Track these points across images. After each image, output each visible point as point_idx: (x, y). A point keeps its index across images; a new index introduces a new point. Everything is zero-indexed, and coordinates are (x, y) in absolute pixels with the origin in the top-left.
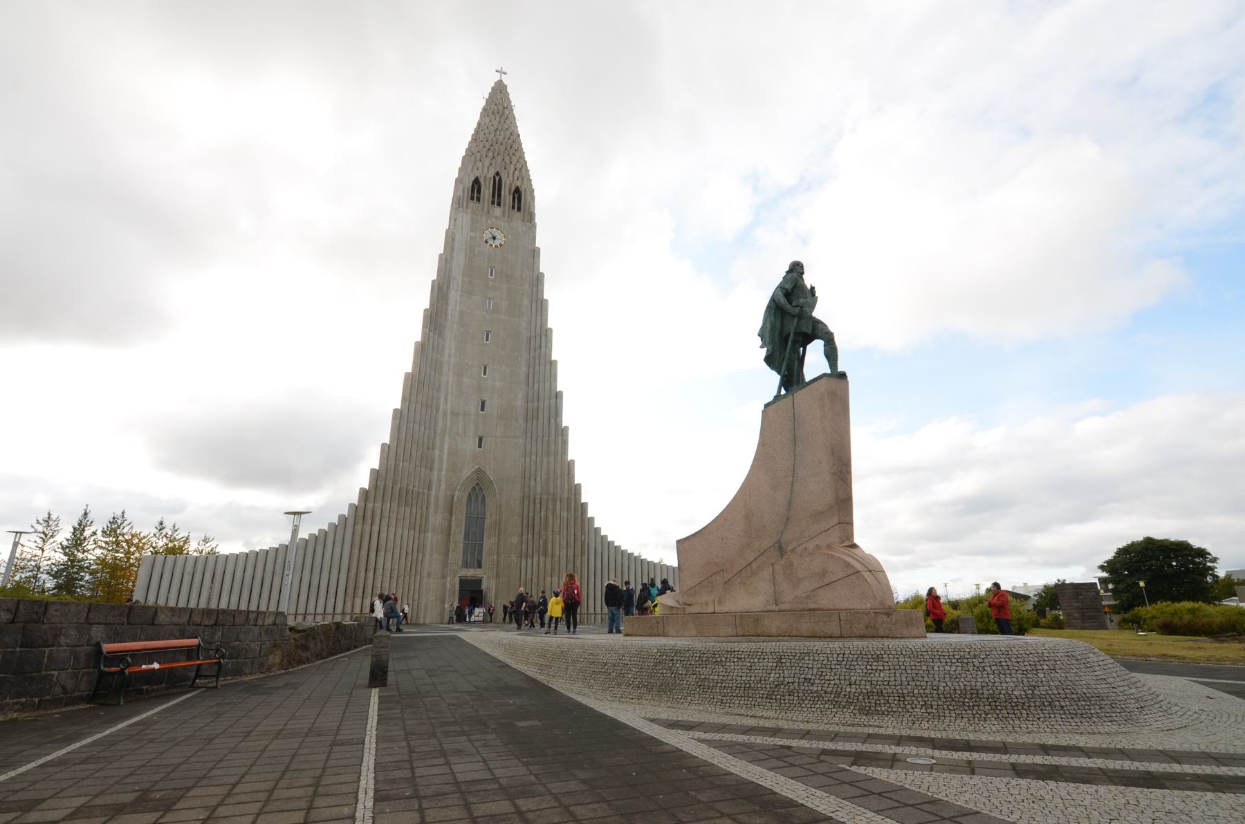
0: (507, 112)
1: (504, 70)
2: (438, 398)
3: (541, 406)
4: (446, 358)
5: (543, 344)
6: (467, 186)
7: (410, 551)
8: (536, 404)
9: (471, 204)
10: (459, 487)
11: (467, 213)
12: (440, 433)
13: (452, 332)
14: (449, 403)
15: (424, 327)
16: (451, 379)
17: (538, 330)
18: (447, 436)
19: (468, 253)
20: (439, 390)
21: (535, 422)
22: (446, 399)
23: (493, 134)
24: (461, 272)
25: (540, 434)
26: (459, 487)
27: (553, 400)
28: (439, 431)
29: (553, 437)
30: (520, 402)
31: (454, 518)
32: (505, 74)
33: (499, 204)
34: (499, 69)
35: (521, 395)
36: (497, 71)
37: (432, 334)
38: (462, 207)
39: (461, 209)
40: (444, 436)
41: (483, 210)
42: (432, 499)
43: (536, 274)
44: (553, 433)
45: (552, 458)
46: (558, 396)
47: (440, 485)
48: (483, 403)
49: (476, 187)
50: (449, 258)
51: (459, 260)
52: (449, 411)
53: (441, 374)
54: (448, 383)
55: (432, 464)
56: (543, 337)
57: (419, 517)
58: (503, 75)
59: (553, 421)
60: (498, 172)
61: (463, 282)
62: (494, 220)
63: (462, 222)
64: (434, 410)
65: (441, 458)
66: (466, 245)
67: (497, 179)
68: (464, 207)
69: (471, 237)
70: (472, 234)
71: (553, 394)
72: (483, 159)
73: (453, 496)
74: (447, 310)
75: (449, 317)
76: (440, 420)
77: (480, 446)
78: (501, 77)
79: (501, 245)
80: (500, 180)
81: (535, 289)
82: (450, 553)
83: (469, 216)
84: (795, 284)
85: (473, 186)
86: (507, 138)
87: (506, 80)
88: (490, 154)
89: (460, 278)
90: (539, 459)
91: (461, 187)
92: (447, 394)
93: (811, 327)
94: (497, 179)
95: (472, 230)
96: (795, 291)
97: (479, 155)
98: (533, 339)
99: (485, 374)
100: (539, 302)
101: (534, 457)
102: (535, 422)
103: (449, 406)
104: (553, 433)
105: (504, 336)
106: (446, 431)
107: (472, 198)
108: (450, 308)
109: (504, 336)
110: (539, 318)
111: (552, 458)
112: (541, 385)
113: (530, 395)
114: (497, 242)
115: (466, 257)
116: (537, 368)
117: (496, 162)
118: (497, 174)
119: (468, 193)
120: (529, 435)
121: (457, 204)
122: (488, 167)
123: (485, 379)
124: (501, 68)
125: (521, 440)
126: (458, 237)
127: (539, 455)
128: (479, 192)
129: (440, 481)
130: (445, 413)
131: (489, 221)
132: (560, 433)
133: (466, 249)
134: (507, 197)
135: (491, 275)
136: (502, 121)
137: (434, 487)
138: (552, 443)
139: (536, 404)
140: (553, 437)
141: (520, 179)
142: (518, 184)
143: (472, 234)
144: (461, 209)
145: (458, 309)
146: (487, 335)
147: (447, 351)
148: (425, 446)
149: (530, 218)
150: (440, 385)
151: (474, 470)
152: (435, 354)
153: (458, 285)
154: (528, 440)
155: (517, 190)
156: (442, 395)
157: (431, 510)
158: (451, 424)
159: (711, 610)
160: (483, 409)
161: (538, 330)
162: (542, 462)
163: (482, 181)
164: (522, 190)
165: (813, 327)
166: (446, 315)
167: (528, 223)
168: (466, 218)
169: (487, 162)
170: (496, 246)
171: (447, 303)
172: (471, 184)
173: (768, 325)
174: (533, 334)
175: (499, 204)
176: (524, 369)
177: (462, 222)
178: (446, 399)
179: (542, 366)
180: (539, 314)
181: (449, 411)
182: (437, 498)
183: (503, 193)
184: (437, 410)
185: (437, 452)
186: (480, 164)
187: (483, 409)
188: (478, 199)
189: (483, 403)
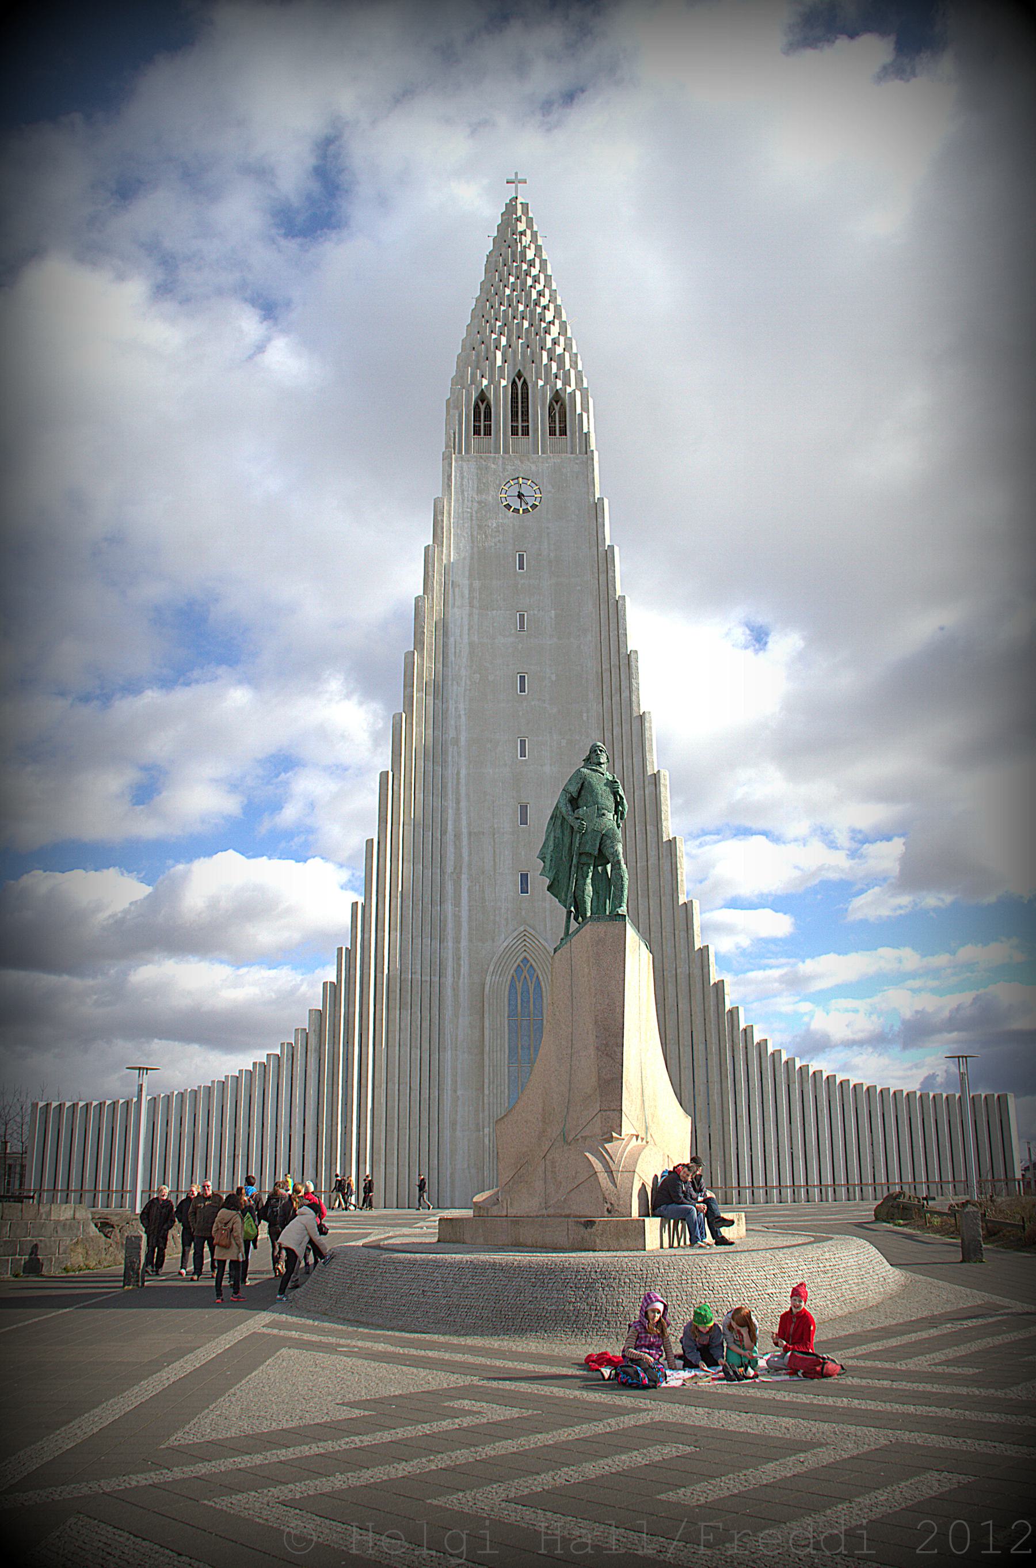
1: (519, 178)
2: (444, 810)
4: (452, 733)
7: (416, 1086)
9: (473, 440)
10: (491, 968)
14: (464, 817)
16: (463, 772)
17: (614, 660)
18: (464, 877)
24: (467, 574)
26: (491, 968)
28: (449, 869)
29: (652, 861)
31: (487, 1024)
38: (460, 452)
40: (459, 878)
42: (449, 992)
44: (652, 853)
47: (459, 965)
48: (524, 809)
49: (482, 407)
52: (465, 831)
53: (444, 764)
54: (458, 779)
55: (443, 929)
57: (426, 1024)
58: (519, 185)
61: (471, 589)
65: (457, 917)
67: (520, 384)
69: (479, 503)
73: (484, 985)
76: (450, 849)
77: (524, 890)
79: (534, 506)
81: (602, 577)
82: (486, 1086)
83: (473, 464)
92: (458, 802)
93: (598, 845)
94: (520, 384)
95: (479, 491)
96: (583, 793)
98: (606, 675)
99: (523, 755)
103: (464, 823)
104: (652, 853)
105: (554, 678)
106: (461, 867)
108: (452, 640)
112: (627, 762)
118: (519, 375)
124: (516, 174)
128: (488, 416)
129: (459, 959)
130: (457, 836)
135: (521, 567)
137: (449, 971)
140: (652, 861)
142: (559, 384)
145: (466, 640)
148: (427, 899)
150: (444, 787)
151: (516, 934)
155: (557, 398)
156: (451, 804)
157: (448, 1013)
158: (470, 854)
159: (504, 1213)
160: (524, 821)
161: (614, 660)
165: (600, 844)
170: (525, 511)
173: (551, 843)
177: (462, 478)
180: (613, 626)
181: (465, 831)
182: (455, 989)
184: (443, 833)
185: (449, 907)
187: (524, 821)
188: (488, 432)
189: (524, 809)
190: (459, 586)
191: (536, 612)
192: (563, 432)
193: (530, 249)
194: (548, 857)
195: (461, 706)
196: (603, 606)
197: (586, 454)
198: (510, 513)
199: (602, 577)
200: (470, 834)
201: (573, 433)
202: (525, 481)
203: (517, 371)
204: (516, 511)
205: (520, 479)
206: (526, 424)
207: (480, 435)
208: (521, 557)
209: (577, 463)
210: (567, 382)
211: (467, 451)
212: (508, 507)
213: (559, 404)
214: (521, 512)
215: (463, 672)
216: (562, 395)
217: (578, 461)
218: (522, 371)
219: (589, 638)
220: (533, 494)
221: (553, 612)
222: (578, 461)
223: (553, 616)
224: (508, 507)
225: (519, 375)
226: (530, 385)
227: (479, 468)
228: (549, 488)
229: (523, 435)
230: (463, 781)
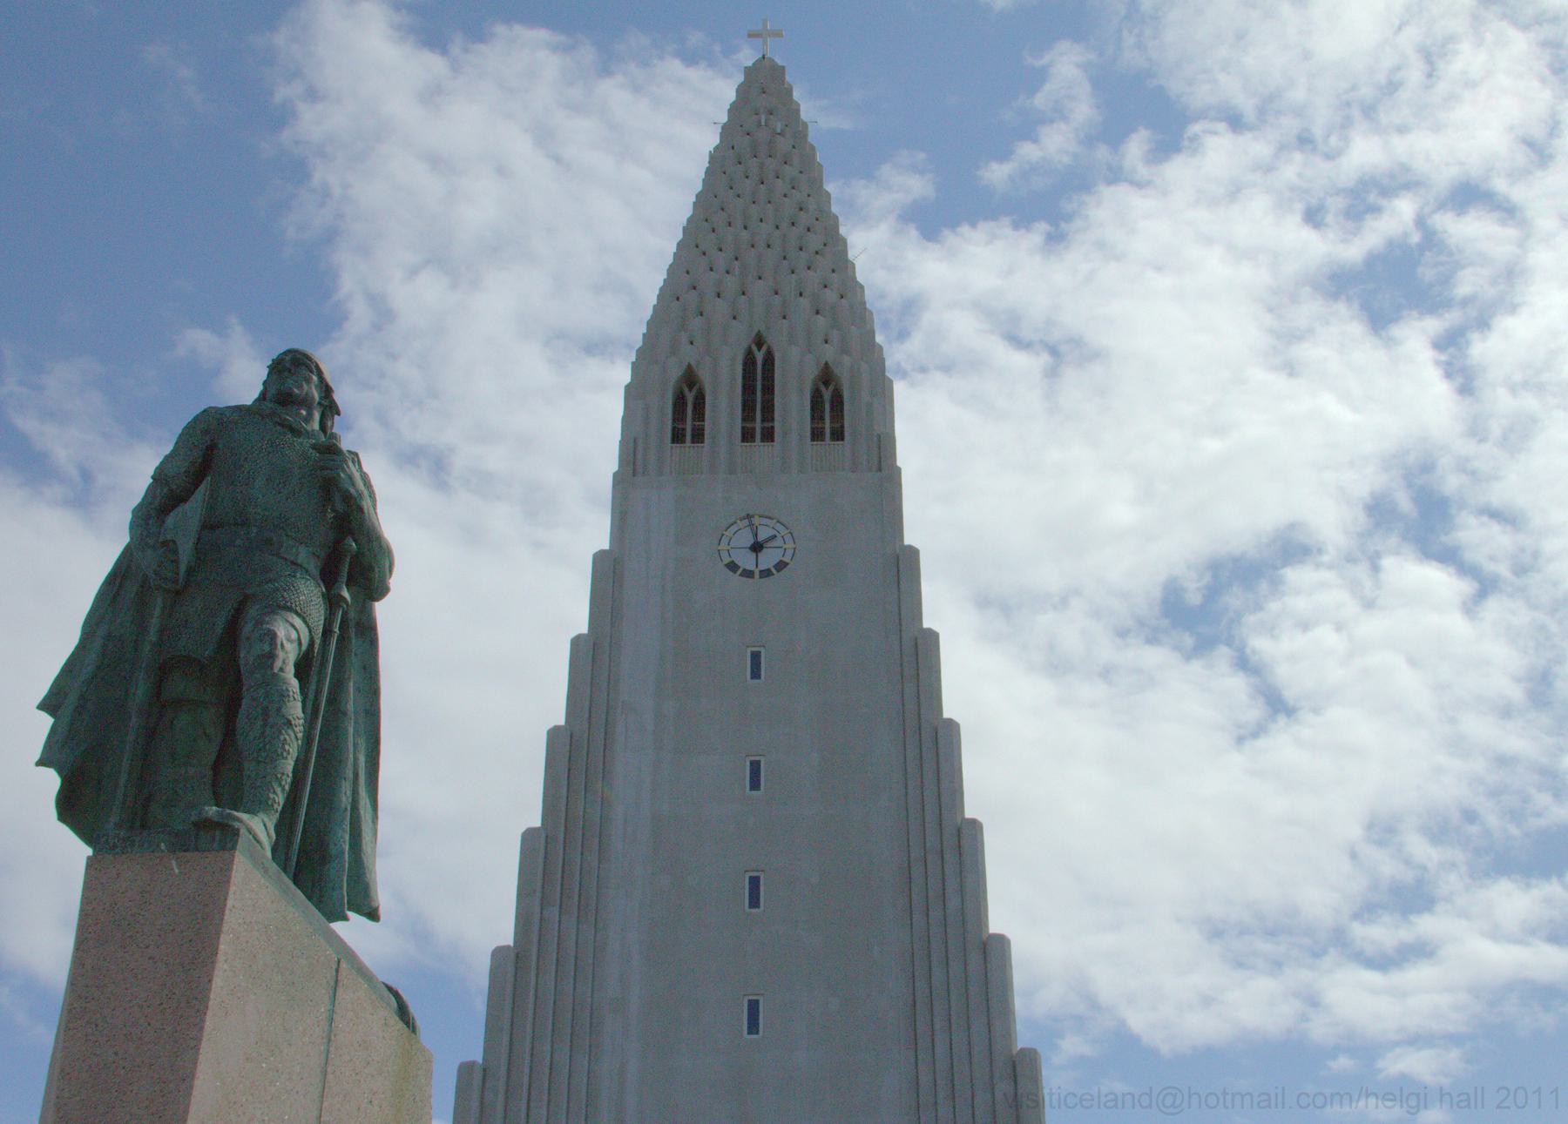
0: (783, 145)
5: (952, 885)
32: (777, 34)
33: (768, 436)
37: (553, 913)
49: (690, 397)
67: (759, 356)
80: (769, 360)
84: (211, 448)
85: (679, 402)
86: (784, 225)
88: (731, 283)
93: (219, 630)
94: (759, 356)
98: (917, 871)
107: (678, 437)
114: (768, 559)
118: (759, 341)
141: (835, 336)
142: (829, 353)
155: (827, 377)
163: (705, 376)
164: (843, 373)
186: (697, 323)
188: (698, 436)
192: (838, 435)
193: (784, 136)
194: (72, 700)
197: (880, 470)
198: (735, 579)
203: (754, 334)
204: (748, 574)
205: (757, 517)
206: (771, 424)
210: (844, 350)
213: (831, 388)
214: (757, 575)
216: (837, 371)
218: (765, 334)
224: (732, 567)
225: (759, 341)
226: (777, 356)
229: (762, 441)
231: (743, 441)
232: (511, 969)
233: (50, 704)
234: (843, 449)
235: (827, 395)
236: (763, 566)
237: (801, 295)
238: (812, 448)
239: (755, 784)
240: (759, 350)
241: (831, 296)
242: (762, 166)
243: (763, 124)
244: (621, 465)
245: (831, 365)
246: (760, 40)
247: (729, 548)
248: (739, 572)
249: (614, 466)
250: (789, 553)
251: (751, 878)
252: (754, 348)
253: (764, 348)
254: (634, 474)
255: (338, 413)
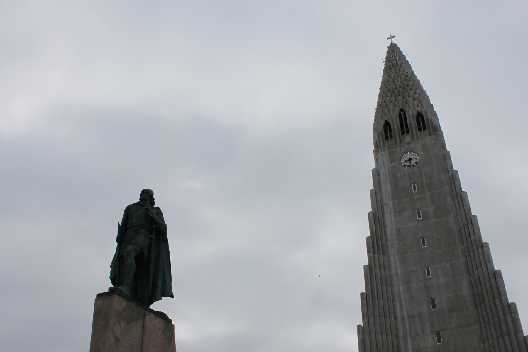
0: (399, 62)
1: (392, 35)
2: (394, 307)
3: (484, 290)
4: (394, 271)
5: (471, 232)
6: (380, 131)
8: (479, 288)
9: (386, 142)
11: (384, 151)
12: (402, 337)
13: (394, 248)
15: (369, 252)
16: (401, 288)
18: (409, 338)
19: (392, 180)
20: (393, 300)
21: (483, 306)
22: (401, 306)
23: (392, 84)
25: (490, 317)
27: (493, 280)
28: (401, 335)
29: (501, 317)
30: (466, 291)
32: (394, 37)
34: (389, 36)
35: (465, 284)
36: (388, 39)
37: (376, 255)
38: (381, 148)
39: (380, 150)
40: (406, 339)
41: (396, 143)
43: (450, 174)
44: (501, 313)
45: (507, 338)
46: (497, 276)
48: (433, 301)
50: (378, 190)
51: (387, 189)
52: (406, 316)
53: (392, 286)
56: (469, 225)
58: (393, 38)
59: (497, 301)
60: (401, 109)
61: (394, 205)
62: (406, 146)
63: (383, 159)
64: (393, 319)
66: (389, 175)
67: (403, 114)
68: (382, 147)
69: (392, 167)
70: (393, 165)
71: (491, 275)
72: (388, 106)
74: (385, 232)
75: (389, 236)
77: (439, 341)
78: (392, 40)
81: (453, 186)
83: (386, 152)
87: (395, 41)
89: (390, 203)
90: (495, 342)
91: (376, 133)
92: (401, 302)
94: (403, 114)
95: (392, 161)
97: (385, 104)
98: (462, 230)
99: (429, 275)
100: (459, 196)
101: (490, 341)
102: (483, 306)
104: (501, 313)
106: (406, 333)
107: (387, 138)
108: (388, 229)
109: (438, 237)
110: (462, 210)
111: (507, 338)
112: (480, 269)
113: (473, 281)
114: (413, 162)
115: (391, 184)
116: (472, 255)
117: (398, 102)
118: (402, 110)
119: (382, 135)
120: (481, 319)
121: (378, 147)
122: (393, 109)
123: (430, 279)
124: (391, 35)
125: (476, 327)
126: (382, 171)
127: (495, 337)
128: (390, 131)
130: (403, 319)
131: (403, 149)
132: (507, 311)
133: (390, 179)
134: (412, 122)
135: (415, 190)
136: (398, 71)
138: (503, 325)
139: (479, 288)
140: (501, 317)
141: (419, 105)
142: (419, 109)
143: (393, 165)
144: (380, 150)
145: (394, 228)
146: (423, 240)
147: (393, 266)
149: (436, 131)
150: (393, 295)
152: (383, 272)
153: (390, 209)
154: (483, 325)
155: (419, 115)
156: (397, 304)
160: (434, 307)
161: (465, 221)
162: (498, 344)
166: (386, 236)
167: (434, 136)
168: (385, 154)
169: (391, 106)
171: (385, 227)
172: (383, 129)
174: (462, 226)
175: (408, 132)
176: (462, 260)
177: (383, 159)
178: (401, 306)
179: (476, 252)
180: (461, 206)
181: (406, 316)
183: (408, 122)
184: (396, 317)
190: (388, 204)
191: (425, 209)
195: (397, 257)
196: (456, 199)
197: (436, 134)
199: (453, 186)
200: (409, 317)
201: (429, 127)
202: (411, 153)
203: (400, 109)
205: (408, 153)
207: (388, 138)
208: (414, 186)
209: (433, 140)
210: (423, 107)
211: (384, 147)
212: (405, 166)
214: (411, 166)
215: (395, 242)
216: (421, 113)
217: (433, 139)
219: (452, 215)
220: (415, 157)
221: (433, 207)
222: (433, 139)
223: (433, 209)
226: (406, 113)
227: (389, 153)
228: (422, 153)
230: (402, 293)
231: (402, 135)
232: (368, 270)
233: (111, 267)
234: (427, 131)
235: (420, 119)
236: (412, 164)
237: (410, 97)
238: (419, 133)
239: (419, 217)
240: (402, 112)
241: (417, 96)
242: (395, 69)
243: (394, 59)
244: (375, 147)
245: (420, 112)
246: (390, 39)
247: (403, 161)
248: (406, 167)
249: (373, 148)
250: (418, 159)
251: (422, 239)
252: (401, 113)
253: (403, 112)
254: (378, 149)
255: (154, 199)
